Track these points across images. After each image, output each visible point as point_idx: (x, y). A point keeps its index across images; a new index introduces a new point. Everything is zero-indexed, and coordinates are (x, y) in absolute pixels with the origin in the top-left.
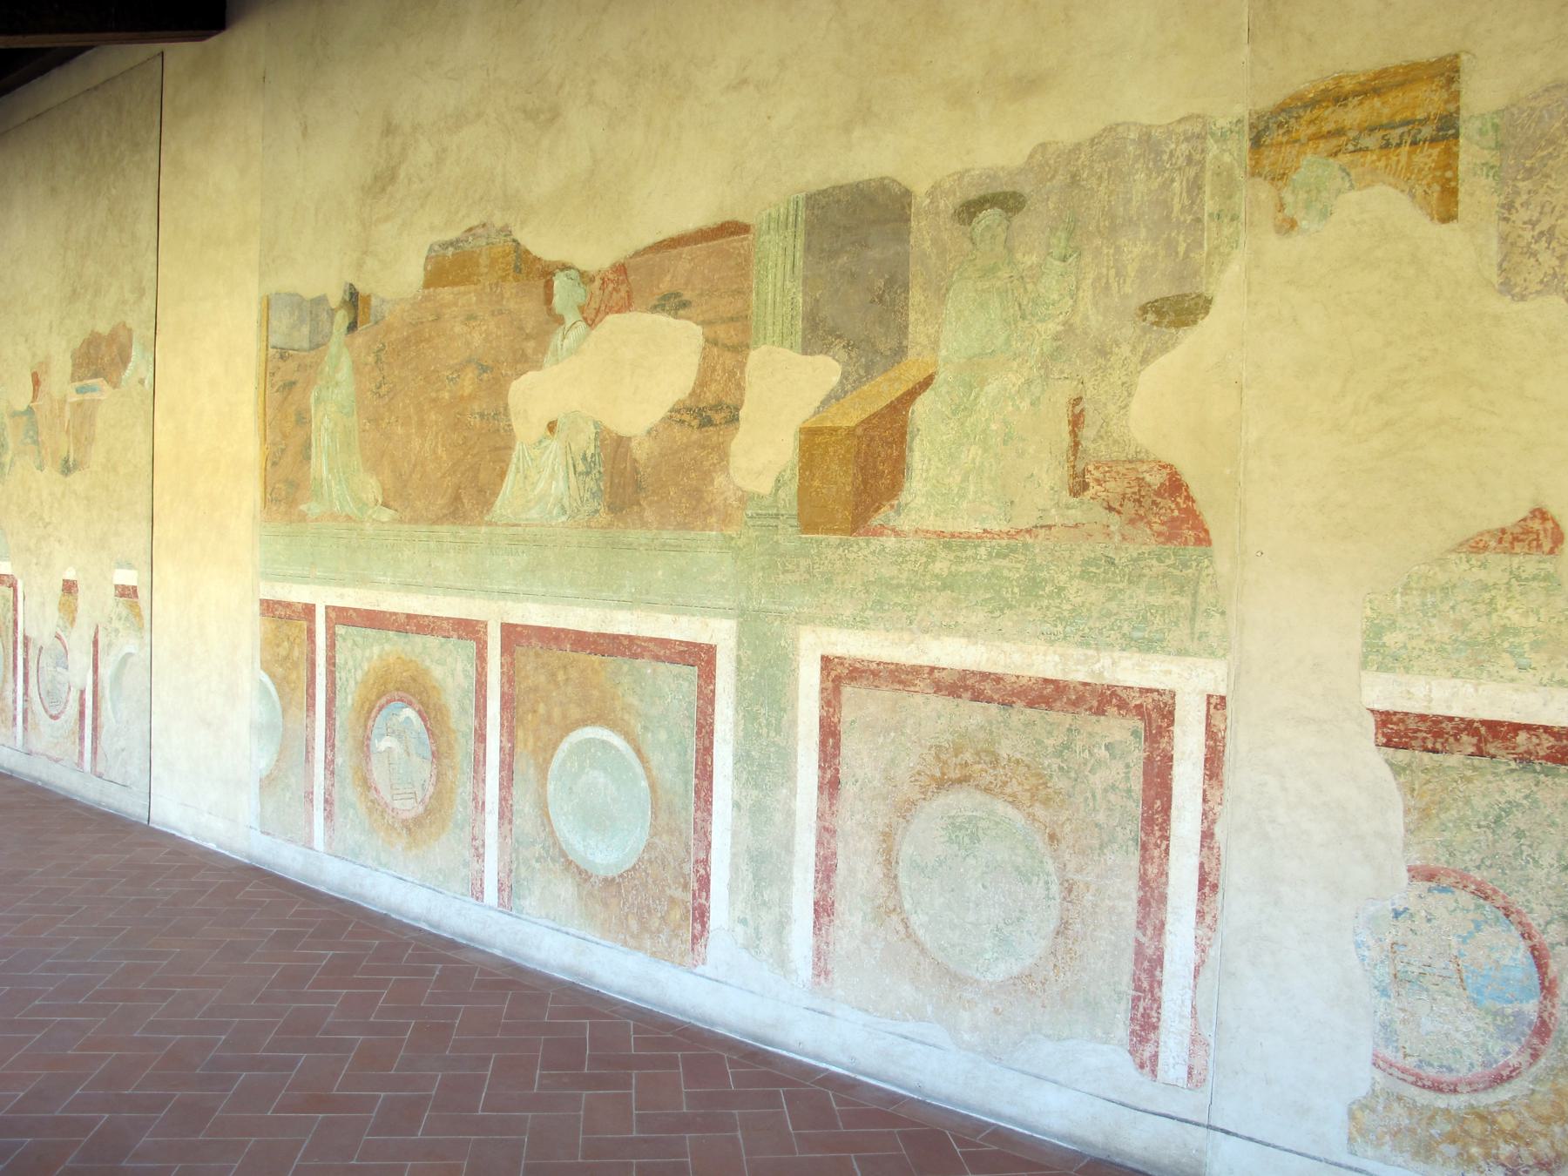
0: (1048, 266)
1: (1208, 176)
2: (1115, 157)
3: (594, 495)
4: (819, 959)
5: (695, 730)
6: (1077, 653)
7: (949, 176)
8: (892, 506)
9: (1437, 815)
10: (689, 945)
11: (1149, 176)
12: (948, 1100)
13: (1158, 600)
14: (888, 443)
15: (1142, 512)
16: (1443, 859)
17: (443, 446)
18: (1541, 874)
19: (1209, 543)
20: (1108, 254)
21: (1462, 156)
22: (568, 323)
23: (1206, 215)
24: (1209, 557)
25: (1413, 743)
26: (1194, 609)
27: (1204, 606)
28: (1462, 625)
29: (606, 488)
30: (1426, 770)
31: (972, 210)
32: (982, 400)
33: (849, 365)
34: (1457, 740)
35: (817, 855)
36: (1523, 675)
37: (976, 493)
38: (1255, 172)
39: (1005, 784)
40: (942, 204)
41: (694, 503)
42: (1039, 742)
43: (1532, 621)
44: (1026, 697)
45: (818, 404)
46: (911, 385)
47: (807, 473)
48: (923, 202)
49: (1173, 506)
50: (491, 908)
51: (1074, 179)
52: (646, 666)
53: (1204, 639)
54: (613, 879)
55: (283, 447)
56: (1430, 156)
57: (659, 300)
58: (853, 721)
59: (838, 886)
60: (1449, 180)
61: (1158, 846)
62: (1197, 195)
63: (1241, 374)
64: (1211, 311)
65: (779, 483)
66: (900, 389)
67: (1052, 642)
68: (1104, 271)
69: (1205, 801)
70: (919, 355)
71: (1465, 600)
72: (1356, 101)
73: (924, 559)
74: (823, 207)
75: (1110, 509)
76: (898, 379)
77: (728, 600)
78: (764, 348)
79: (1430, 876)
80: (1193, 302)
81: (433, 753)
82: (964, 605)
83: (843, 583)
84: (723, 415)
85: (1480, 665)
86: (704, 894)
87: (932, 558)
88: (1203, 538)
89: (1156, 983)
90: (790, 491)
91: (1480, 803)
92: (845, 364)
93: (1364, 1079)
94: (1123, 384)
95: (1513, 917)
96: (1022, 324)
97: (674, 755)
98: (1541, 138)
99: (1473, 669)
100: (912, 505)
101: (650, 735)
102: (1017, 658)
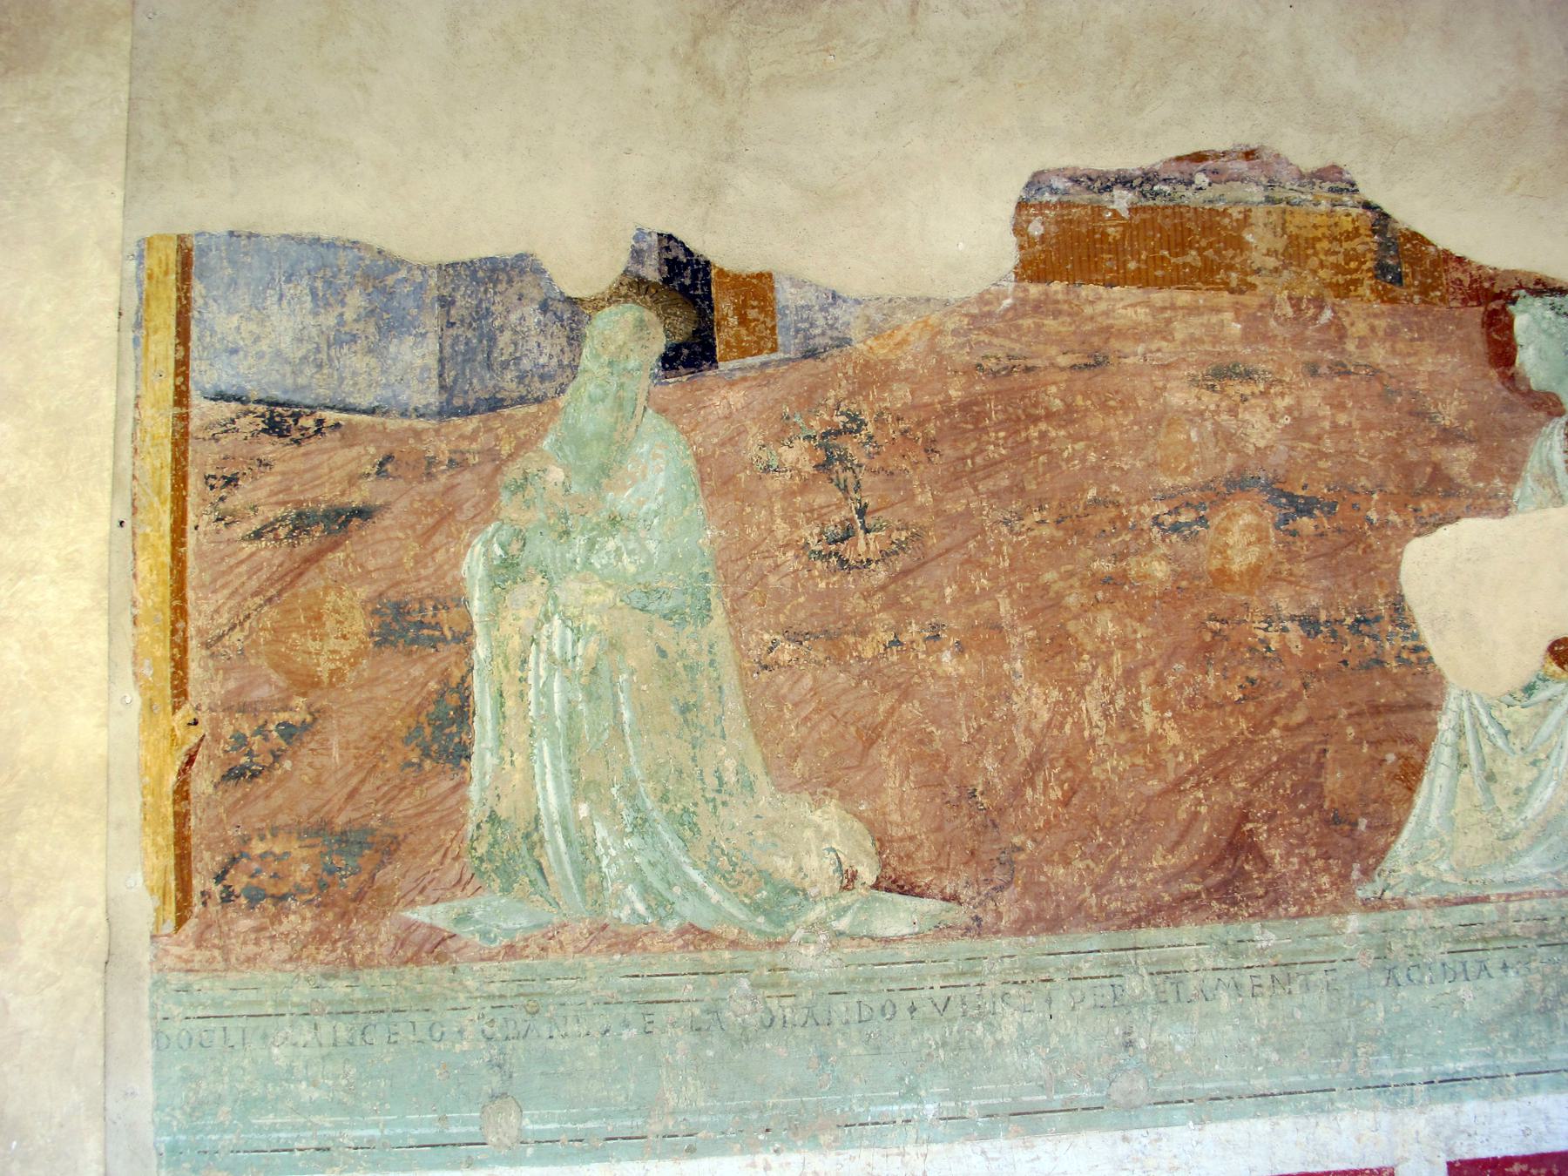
17: (1161, 705)
55: (296, 718)
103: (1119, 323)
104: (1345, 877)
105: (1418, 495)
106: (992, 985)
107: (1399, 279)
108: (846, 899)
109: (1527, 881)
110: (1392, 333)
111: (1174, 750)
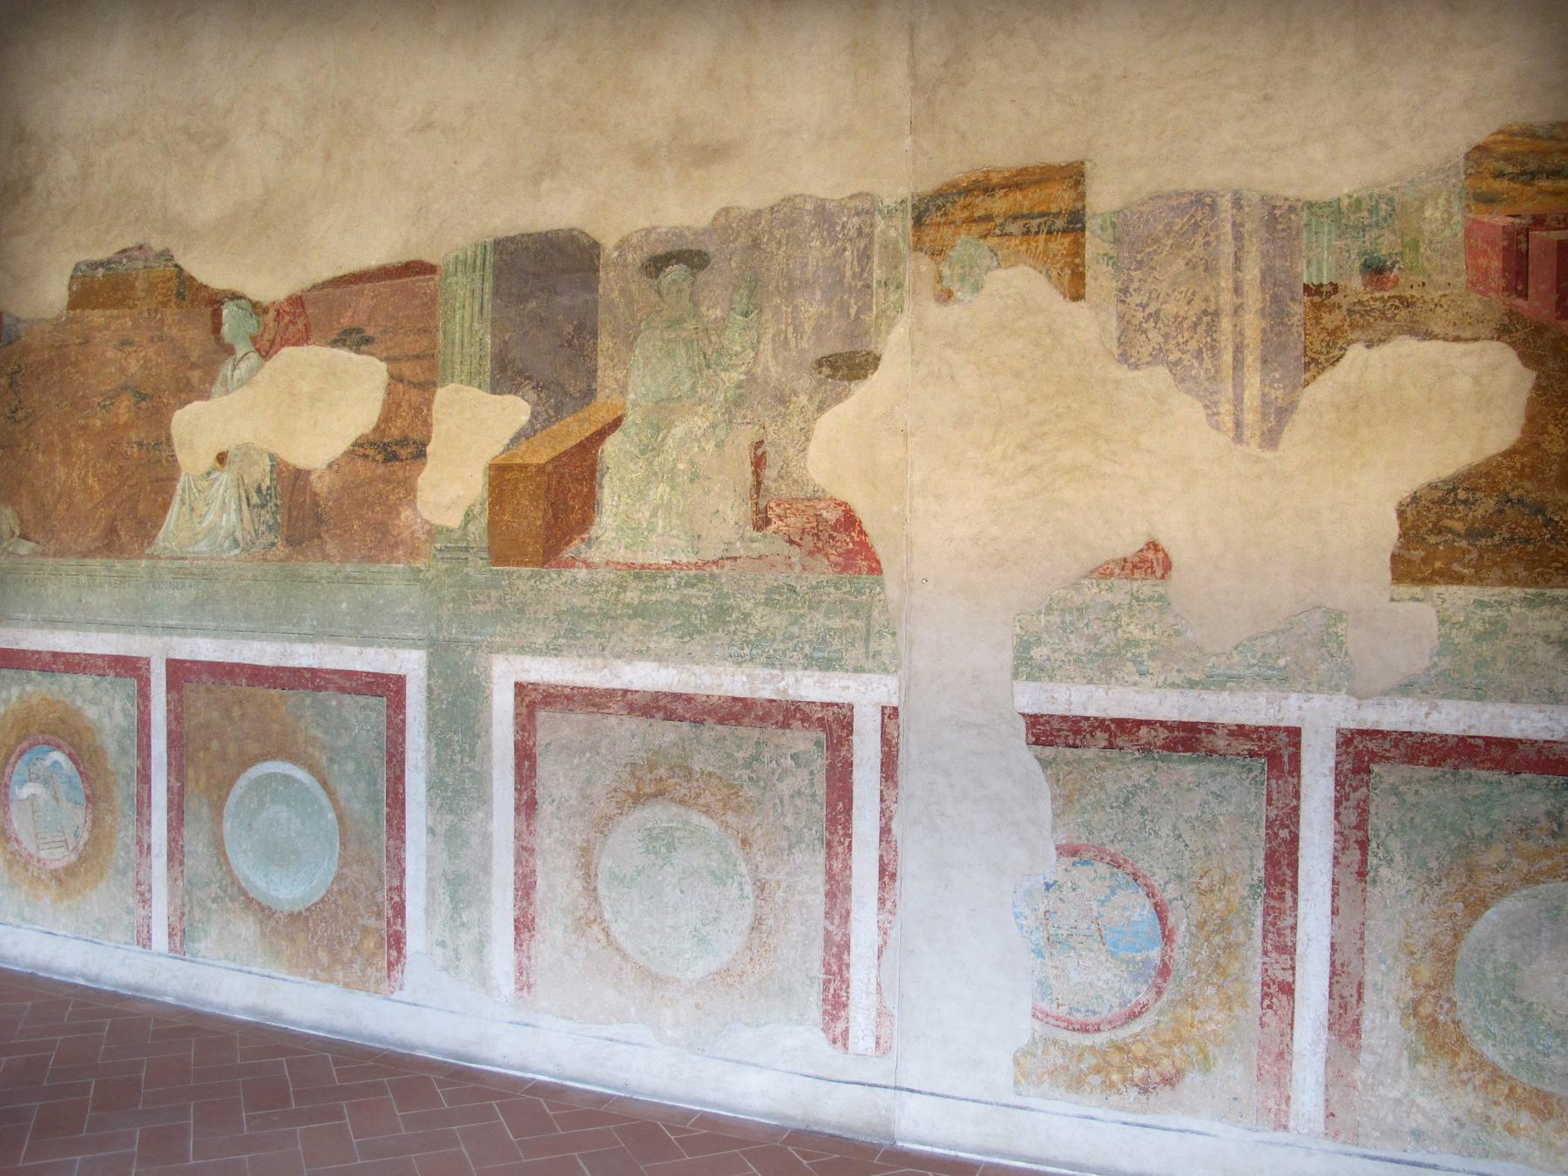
0: (731, 320)
1: (876, 246)
2: (793, 225)
3: (270, 528)
4: (521, 974)
5: (385, 759)
6: (763, 673)
7: (636, 232)
8: (583, 540)
9: (1078, 800)
10: (385, 973)
11: (823, 244)
12: (655, 1094)
13: (836, 623)
14: (577, 480)
15: (820, 545)
16: (1084, 837)
17: (94, 475)
18: (1161, 843)
19: (880, 572)
20: (786, 312)
21: (1087, 246)
22: (239, 354)
23: (874, 281)
24: (882, 585)
25: (1058, 740)
26: (868, 631)
27: (878, 628)
28: (1095, 639)
29: (283, 517)
30: (1068, 763)
31: (659, 265)
32: (670, 441)
33: (537, 405)
34: (1092, 736)
35: (515, 874)
36: (1143, 679)
37: (664, 527)
38: (917, 247)
39: (698, 795)
40: (630, 257)
41: (379, 536)
42: (730, 755)
43: (1149, 635)
44: (716, 714)
45: (507, 441)
46: (600, 426)
47: (497, 508)
48: (609, 255)
49: (848, 540)
50: (160, 954)
51: (756, 243)
52: (332, 699)
53: (878, 657)
54: (300, 913)
56: (1062, 244)
57: (340, 334)
58: (548, 744)
59: (538, 902)
60: (1078, 266)
61: (841, 843)
62: (867, 263)
63: (906, 424)
64: (880, 367)
65: (468, 517)
66: (589, 430)
67: (739, 664)
68: (783, 327)
69: (882, 800)
70: (608, 397)
71: (1096, 618)
72: (1002, 192)
73: (615, 589)
74: (512, 253)
75: (791, 542)
76: (587, 420)
77: (415, 631)
78: (452, 386)
79: (1074, 852)
80: (863, 359)
81: (88, 798)
82: (654, 632)
83: (535, 612)
84: (409, 450)
85: (1109, 673)
86: (399, 920)
87: (623, 588)
88: (875, 568)
89: (844, 966)
90: (479, 527)
91: (1112, 788)
92: (534, 404)
93: (1025, 1029)
94: (801, 429)
95: (1140, 880)
96: (706, 372)
97: (363, 784)
98: (1148, 237)
99: (1104, 676)
100: (603, 538)
101: (336, 766)
102: (707, 679)
103: (94, 325)
104: (142, 544)
105: (182, 391)
106: (47, 574)
107: (183, 299)
108: (12, 540)
109: (201, 552)
110: (180, 322)
111: (97, 492)
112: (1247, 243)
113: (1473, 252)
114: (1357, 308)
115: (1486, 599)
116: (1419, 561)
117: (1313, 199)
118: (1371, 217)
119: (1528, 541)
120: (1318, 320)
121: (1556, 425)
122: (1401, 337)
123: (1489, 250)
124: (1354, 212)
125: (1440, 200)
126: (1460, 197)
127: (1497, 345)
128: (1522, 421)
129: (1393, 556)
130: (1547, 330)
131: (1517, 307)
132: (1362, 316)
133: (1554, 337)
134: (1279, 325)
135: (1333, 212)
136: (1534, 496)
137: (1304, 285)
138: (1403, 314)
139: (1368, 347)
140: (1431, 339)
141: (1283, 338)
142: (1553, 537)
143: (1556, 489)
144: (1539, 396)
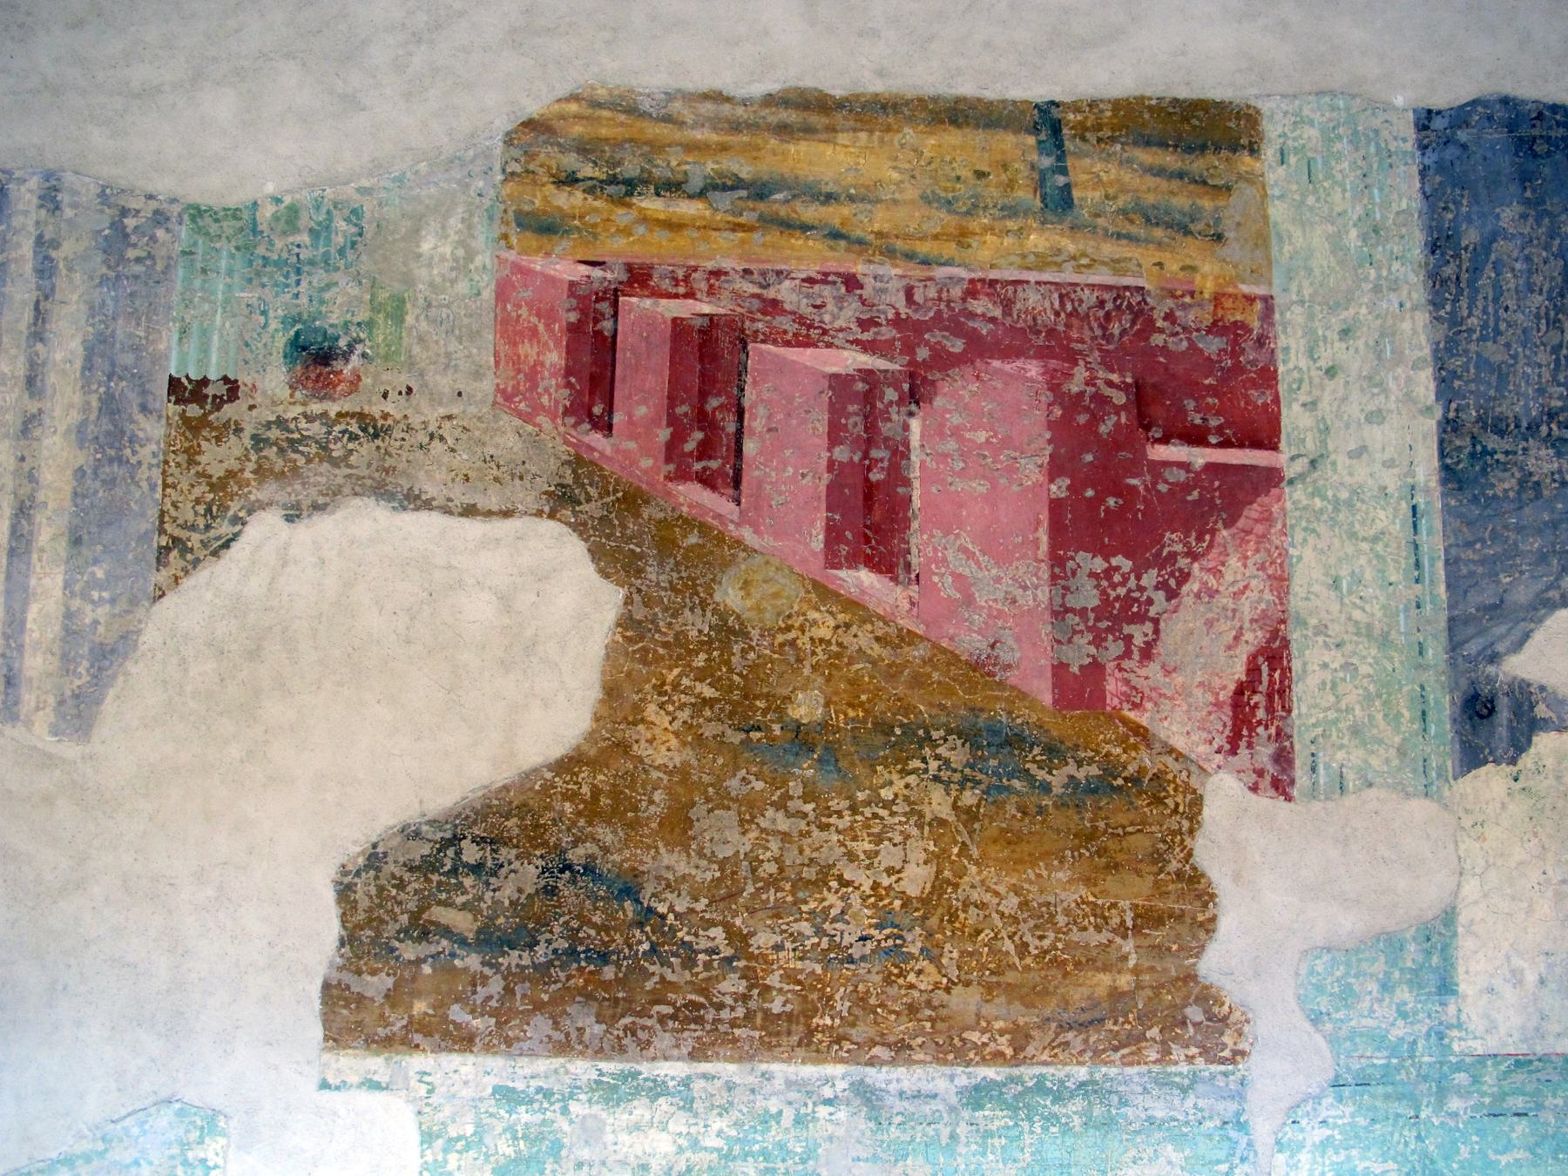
112: (61, 282)
113: (509, 330)
114: (274, 433)
115: (520, 1085)
116: (380, 999)
117: (204, 201)
118: (315, 246)
119: (604, 958)
120: (192, 454)
121: (661, 706)
122: (357, 501)
123: (541, 327)
124: (284, 233)
125: (452, 221)
126: (491, 218)
127: (553, 526)
128: (596, 693)
129: (326, 986)
130: (647, 502)
131: (592, 449)
132: (281, 450)
133: (661, 515)
134: (111, 461)
135: (242, 229)
136: (616, 857)
137: (171, 378)
138: (365, 450)
139: (289, 519)
140: (417, 509)
141: (119, 492)
142: (654, 949)
143: (660, 844)
144: (629, 640)
